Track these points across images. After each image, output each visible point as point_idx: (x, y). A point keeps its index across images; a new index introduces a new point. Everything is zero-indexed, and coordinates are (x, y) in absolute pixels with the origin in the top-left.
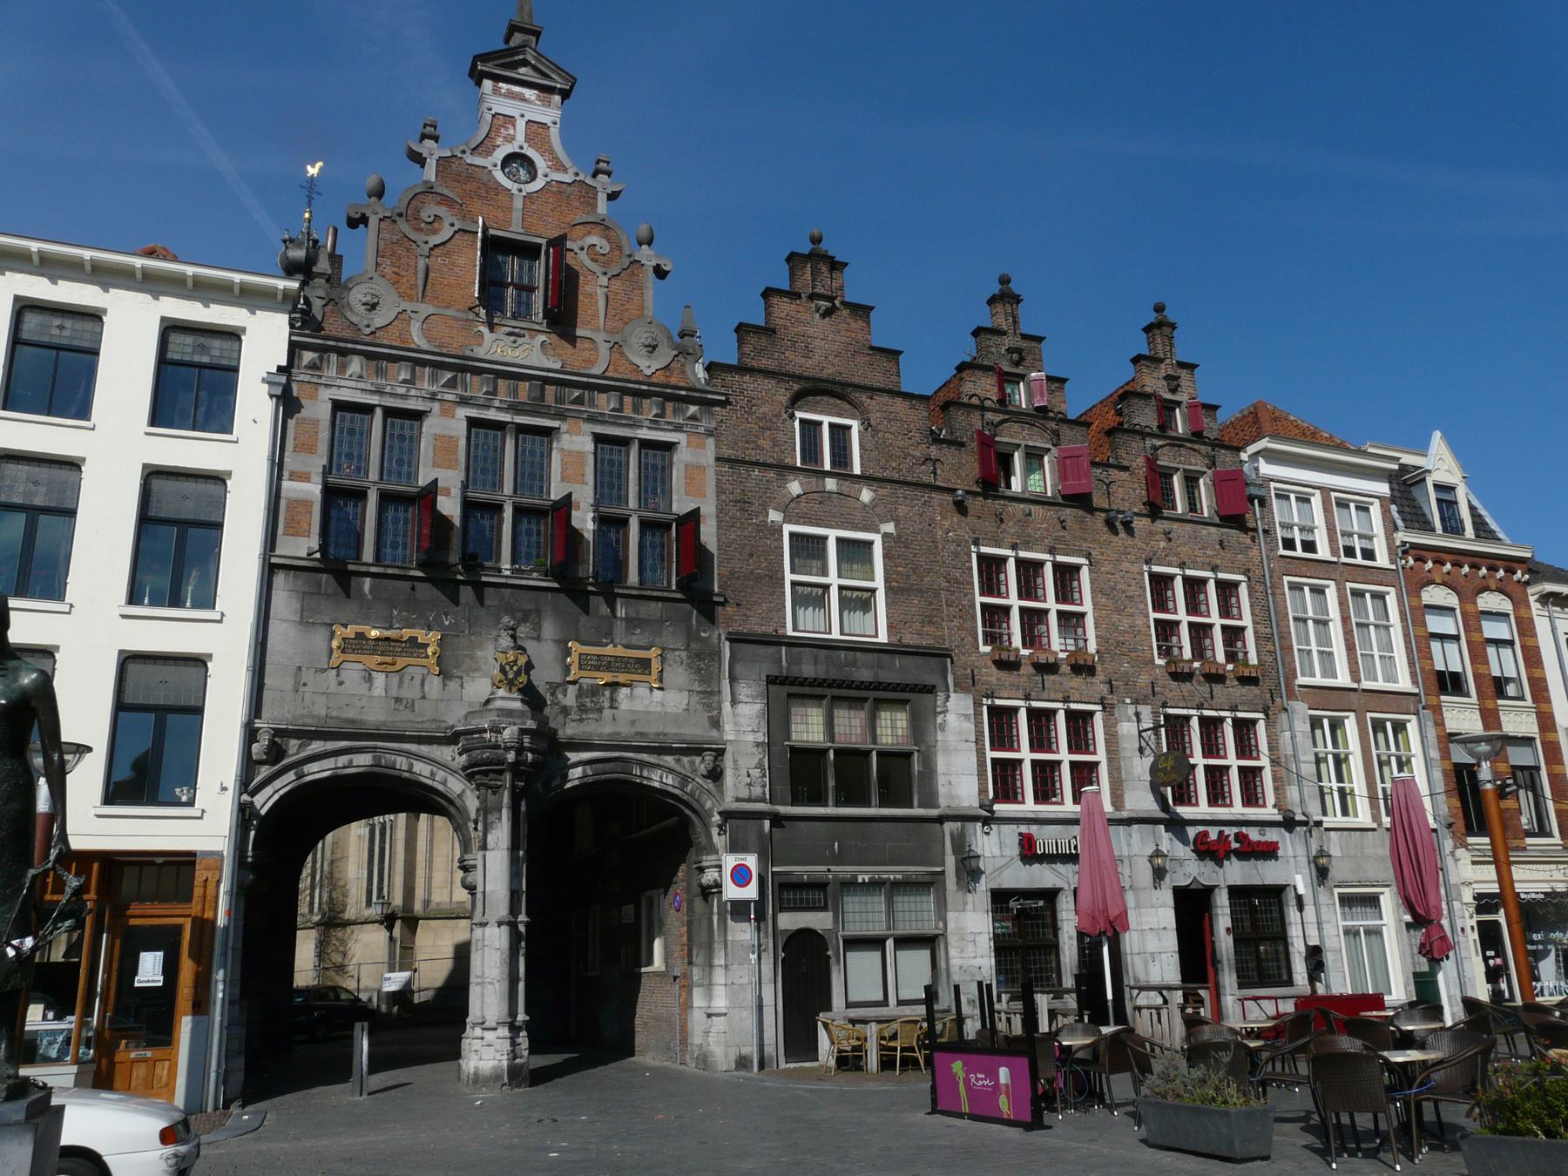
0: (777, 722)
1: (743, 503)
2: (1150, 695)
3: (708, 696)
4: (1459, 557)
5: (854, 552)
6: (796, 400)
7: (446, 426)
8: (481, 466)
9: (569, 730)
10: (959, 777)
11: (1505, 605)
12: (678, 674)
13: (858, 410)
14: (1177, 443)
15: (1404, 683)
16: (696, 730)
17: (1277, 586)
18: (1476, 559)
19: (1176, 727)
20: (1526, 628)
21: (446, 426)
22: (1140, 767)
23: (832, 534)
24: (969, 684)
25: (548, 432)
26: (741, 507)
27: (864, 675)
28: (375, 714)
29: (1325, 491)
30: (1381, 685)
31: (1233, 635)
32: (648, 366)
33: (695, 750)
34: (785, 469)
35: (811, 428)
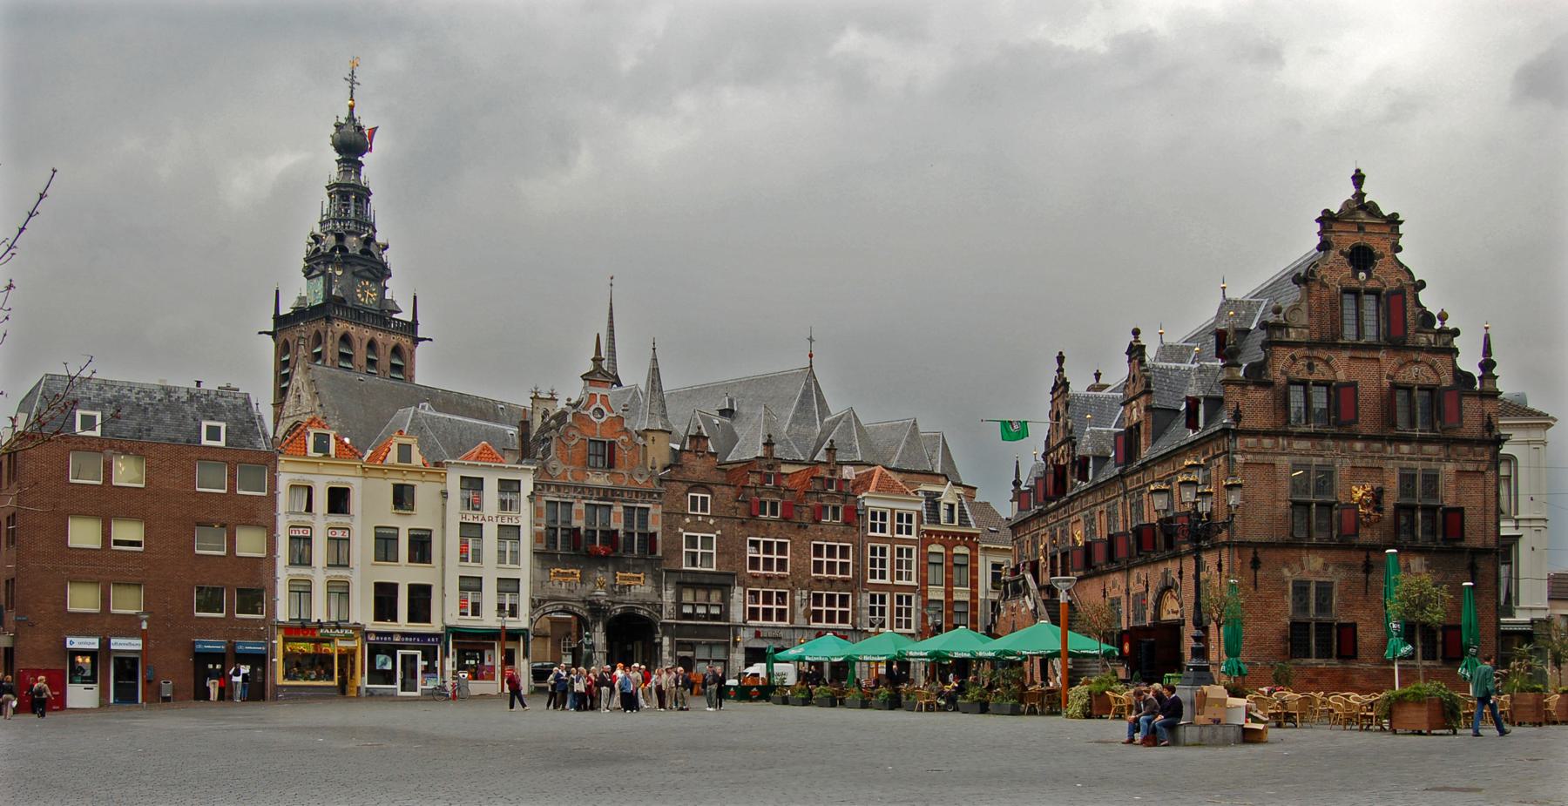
0: (679, 596)
1: (670, 527)
2: (809, 588)
3: (658, 588)
4: (947, 534)
5: (707, 542)
6: (691, 489)
7: (580, 506)
8: (591, 519)
9: (617, 598)
10: (737, 614)
11: (967, 551)
12: (649, 581)
13: (711, 492)
14: (831, 496)
15: (913, 582)
16: (654, 598)
17: (864, 548)
18: (955, 535)
19: (817, 599)
20: (974, 560)
21: (580, 506)
22: (800, 611)
23: (699, 535)
24: (743, 584)
25: (610, 507)
26: (669, 527)
27: (707, 581)
28: (563, 595)
29: (893, 510)
30: (904, 582)
31: (844, 566)
32: (641, 481)
33: (654, 604)
34: (685, 515)
35: (694, 499)
